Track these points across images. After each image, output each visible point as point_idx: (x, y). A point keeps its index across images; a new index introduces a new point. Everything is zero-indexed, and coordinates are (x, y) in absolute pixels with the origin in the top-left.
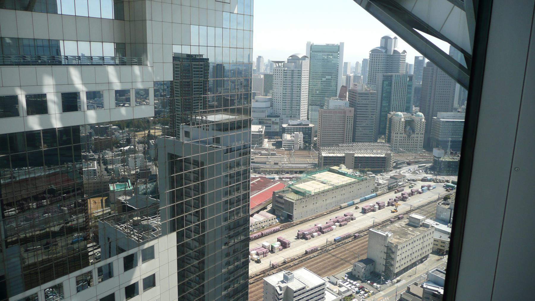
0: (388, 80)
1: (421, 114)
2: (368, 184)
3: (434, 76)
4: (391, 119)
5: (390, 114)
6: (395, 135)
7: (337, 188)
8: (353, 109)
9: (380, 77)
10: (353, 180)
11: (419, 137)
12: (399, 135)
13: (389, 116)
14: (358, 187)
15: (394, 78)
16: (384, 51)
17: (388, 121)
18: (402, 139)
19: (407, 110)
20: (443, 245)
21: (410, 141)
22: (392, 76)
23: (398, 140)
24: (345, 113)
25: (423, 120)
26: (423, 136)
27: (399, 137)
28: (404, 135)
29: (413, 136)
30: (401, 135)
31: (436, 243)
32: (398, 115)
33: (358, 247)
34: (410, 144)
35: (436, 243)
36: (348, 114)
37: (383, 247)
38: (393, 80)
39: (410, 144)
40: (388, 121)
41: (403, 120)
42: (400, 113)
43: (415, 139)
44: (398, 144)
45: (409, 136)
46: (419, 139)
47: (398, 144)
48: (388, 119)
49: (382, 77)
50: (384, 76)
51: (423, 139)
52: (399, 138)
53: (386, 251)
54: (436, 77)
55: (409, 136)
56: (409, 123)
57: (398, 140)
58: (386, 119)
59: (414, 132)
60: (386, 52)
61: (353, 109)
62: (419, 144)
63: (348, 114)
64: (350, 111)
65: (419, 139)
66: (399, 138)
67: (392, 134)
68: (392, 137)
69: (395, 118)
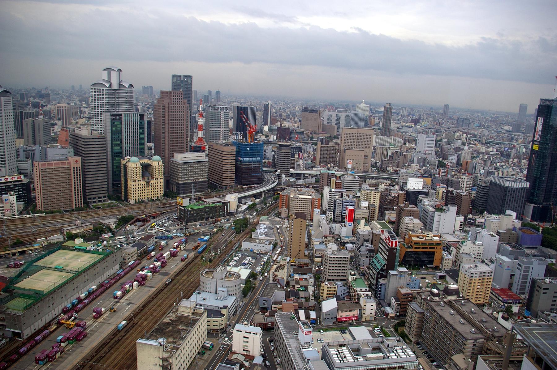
0: (116, 118)
1: (157, 157)
2: (115, 258)
3: (167, 114)
4: (125, 165)
5: (124, 159)
6: (132, 183)
7: (79, 274)
8: (80, 158)
9: (108, 118)
10: (95, 258)
11: (158, 183)
12: (137, 183)
13: (123, 162)
14: (104, 265)
15: (123, 118)
16: (108, 85)
17: (122, 168)
18: (141, 186)
19: (141, 153)
20: (215, 323)
21: (150, 188)
22: (121, 115)
23: (137, 188)
24: (69, 163)
25: (161, 163)
26: (163, 180)
27: (137, 185)
28: (144, 182)
29: (152, 182)
30: (139, 182)
31: (209, 323)
32: (134, 162)
33: (121, 356)
34: (150, 191)
35: (209, 323)
36: (73, 165)
37: (157, 359)
38: (123, 120)
39: (150, 191)
40: (122, 168)
41: (139, 165)
42: (134, 159)
43: (155, 185)
44: (137, 192)
45: (148, 183)
46: (159, 184)
47: (137, 192)
48: (122, 166)
49: (110, 117)
50: (111, 115)
51: (163, 184)
52: (137, 187)
53: (161, 364)
54: (169, 114)
55: (148, 183)
56: (146, 168)
57: (137, 188)
58: (120, 163)
59: (152, 178)
60: (110, 86)
61: (80, 158)
62: (159, 190)
63: (73, 165)
64: (77, 161)
65: (159, 184)
66: (137, 187)
67: (129, 183)
68: (129, 186)
69: (131, 165)
